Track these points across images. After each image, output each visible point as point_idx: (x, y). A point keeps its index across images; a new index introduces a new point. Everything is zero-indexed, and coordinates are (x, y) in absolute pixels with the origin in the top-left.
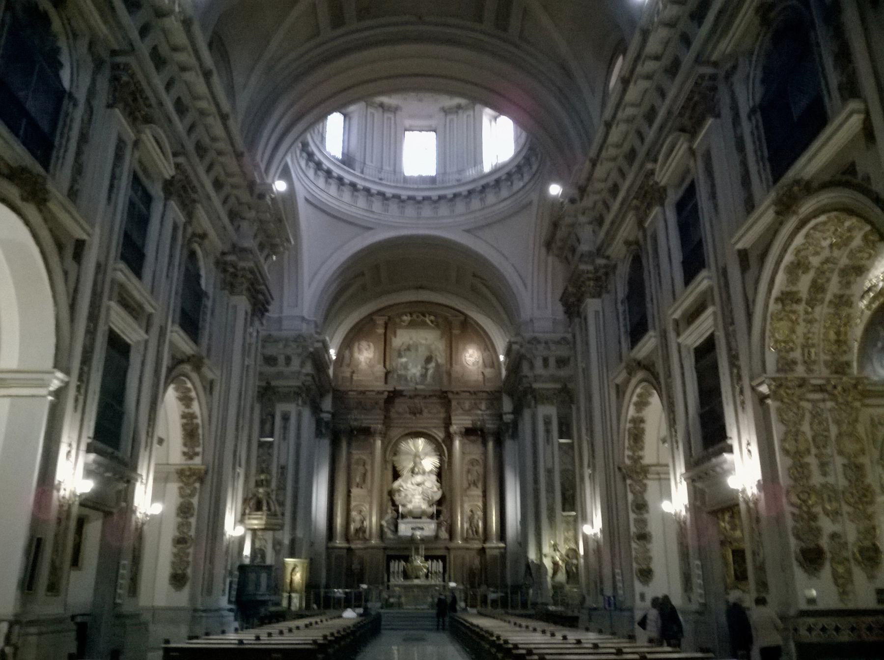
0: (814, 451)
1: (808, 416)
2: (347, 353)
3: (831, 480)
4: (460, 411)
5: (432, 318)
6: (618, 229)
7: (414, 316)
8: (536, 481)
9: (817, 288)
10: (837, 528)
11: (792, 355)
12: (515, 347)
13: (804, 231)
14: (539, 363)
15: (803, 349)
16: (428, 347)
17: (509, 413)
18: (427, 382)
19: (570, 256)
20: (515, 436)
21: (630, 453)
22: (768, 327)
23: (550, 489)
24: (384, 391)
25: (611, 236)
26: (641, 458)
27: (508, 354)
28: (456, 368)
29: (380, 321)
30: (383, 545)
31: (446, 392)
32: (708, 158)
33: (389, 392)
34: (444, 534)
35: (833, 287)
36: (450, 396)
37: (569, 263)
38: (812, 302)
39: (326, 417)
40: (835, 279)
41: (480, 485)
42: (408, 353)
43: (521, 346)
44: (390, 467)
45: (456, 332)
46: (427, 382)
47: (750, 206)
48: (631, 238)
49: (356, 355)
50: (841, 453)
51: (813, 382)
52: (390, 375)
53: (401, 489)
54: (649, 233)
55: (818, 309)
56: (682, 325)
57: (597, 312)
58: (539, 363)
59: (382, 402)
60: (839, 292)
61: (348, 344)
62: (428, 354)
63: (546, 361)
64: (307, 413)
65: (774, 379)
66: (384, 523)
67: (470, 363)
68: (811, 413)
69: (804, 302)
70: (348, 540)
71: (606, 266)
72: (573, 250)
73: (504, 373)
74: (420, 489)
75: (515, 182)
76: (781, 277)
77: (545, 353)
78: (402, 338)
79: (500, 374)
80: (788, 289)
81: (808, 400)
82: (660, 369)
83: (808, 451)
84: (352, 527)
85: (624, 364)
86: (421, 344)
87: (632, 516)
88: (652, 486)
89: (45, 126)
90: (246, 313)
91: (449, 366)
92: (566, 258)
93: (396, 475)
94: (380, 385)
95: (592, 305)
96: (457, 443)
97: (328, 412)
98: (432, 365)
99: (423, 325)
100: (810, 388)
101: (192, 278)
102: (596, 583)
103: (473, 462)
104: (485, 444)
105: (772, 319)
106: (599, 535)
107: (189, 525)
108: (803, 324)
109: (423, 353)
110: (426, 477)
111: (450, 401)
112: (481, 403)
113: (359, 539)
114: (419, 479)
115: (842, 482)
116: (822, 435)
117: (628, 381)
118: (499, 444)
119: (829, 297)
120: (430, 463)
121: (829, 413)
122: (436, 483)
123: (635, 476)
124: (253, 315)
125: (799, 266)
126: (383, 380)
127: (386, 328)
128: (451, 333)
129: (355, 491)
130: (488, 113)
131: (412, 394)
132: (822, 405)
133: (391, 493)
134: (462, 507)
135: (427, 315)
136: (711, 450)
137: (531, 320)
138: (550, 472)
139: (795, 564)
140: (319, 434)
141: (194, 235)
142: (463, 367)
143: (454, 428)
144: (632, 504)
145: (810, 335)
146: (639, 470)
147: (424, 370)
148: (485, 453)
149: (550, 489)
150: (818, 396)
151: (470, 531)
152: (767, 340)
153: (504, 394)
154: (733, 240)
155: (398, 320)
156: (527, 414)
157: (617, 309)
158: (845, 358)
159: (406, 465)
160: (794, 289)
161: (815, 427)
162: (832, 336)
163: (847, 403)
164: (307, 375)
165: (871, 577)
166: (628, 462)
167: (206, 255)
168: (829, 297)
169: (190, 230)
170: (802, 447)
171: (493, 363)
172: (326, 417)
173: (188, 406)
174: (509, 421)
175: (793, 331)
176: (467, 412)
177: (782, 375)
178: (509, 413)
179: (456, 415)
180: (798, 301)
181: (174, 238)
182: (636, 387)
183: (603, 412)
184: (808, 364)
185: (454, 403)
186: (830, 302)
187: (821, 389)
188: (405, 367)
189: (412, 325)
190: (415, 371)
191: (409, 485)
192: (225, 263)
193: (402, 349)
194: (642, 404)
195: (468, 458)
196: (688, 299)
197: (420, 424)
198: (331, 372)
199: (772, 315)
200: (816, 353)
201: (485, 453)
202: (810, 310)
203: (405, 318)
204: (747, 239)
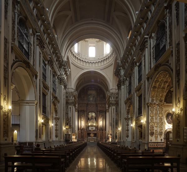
0: (155, 116)
10: (157, 129)
50: (159, 116)
57: (123, 88)
83: (154, 116)
88: (130, 121)
138: (114, 118)
156: (110, 107)
165: (161, 137)
170: (153, 115)
187: (158, 105)
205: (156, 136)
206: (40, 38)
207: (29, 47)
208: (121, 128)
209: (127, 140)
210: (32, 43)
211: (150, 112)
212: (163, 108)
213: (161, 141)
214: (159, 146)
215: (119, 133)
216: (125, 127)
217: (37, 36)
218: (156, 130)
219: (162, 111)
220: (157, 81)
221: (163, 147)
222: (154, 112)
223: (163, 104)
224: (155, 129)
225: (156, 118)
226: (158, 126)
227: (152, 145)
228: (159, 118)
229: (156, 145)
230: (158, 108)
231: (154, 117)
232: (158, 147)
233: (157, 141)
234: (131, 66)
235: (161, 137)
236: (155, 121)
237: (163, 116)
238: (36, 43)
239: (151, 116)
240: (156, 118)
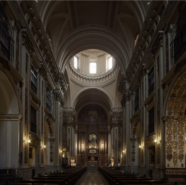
0: (173, 133)
3: (176, 140)
10: (175, 151)
34: (97, 153)
50: (178, 134)
107: (52, 150)
115: (178, 141)
139: (166, 158)
150: (176, 121)
165: (181, 161)
170: (171, 133)
205: (175, 160)
206: (27, 35)
211: (167, 128)
212: (184, 123)
214: (180, 174)
217: (22, 33)
218: (175, 152)
219: (183, 126)
222: (172, 128)
223: (184, 118)
224: (173, 150)
225: (175, 136)
226: (178, 146)
227: (170, 172)
228: (178, 136)
229: (176, 172)
230: (178, 123)
231: (171, 135)
232: (178, 174)
233: (176, 167)
235: (181, 161)
236: (173, 140)
237: (183, 133)
238: (21, 41)
239: (167, 134)
240: (175, 136)
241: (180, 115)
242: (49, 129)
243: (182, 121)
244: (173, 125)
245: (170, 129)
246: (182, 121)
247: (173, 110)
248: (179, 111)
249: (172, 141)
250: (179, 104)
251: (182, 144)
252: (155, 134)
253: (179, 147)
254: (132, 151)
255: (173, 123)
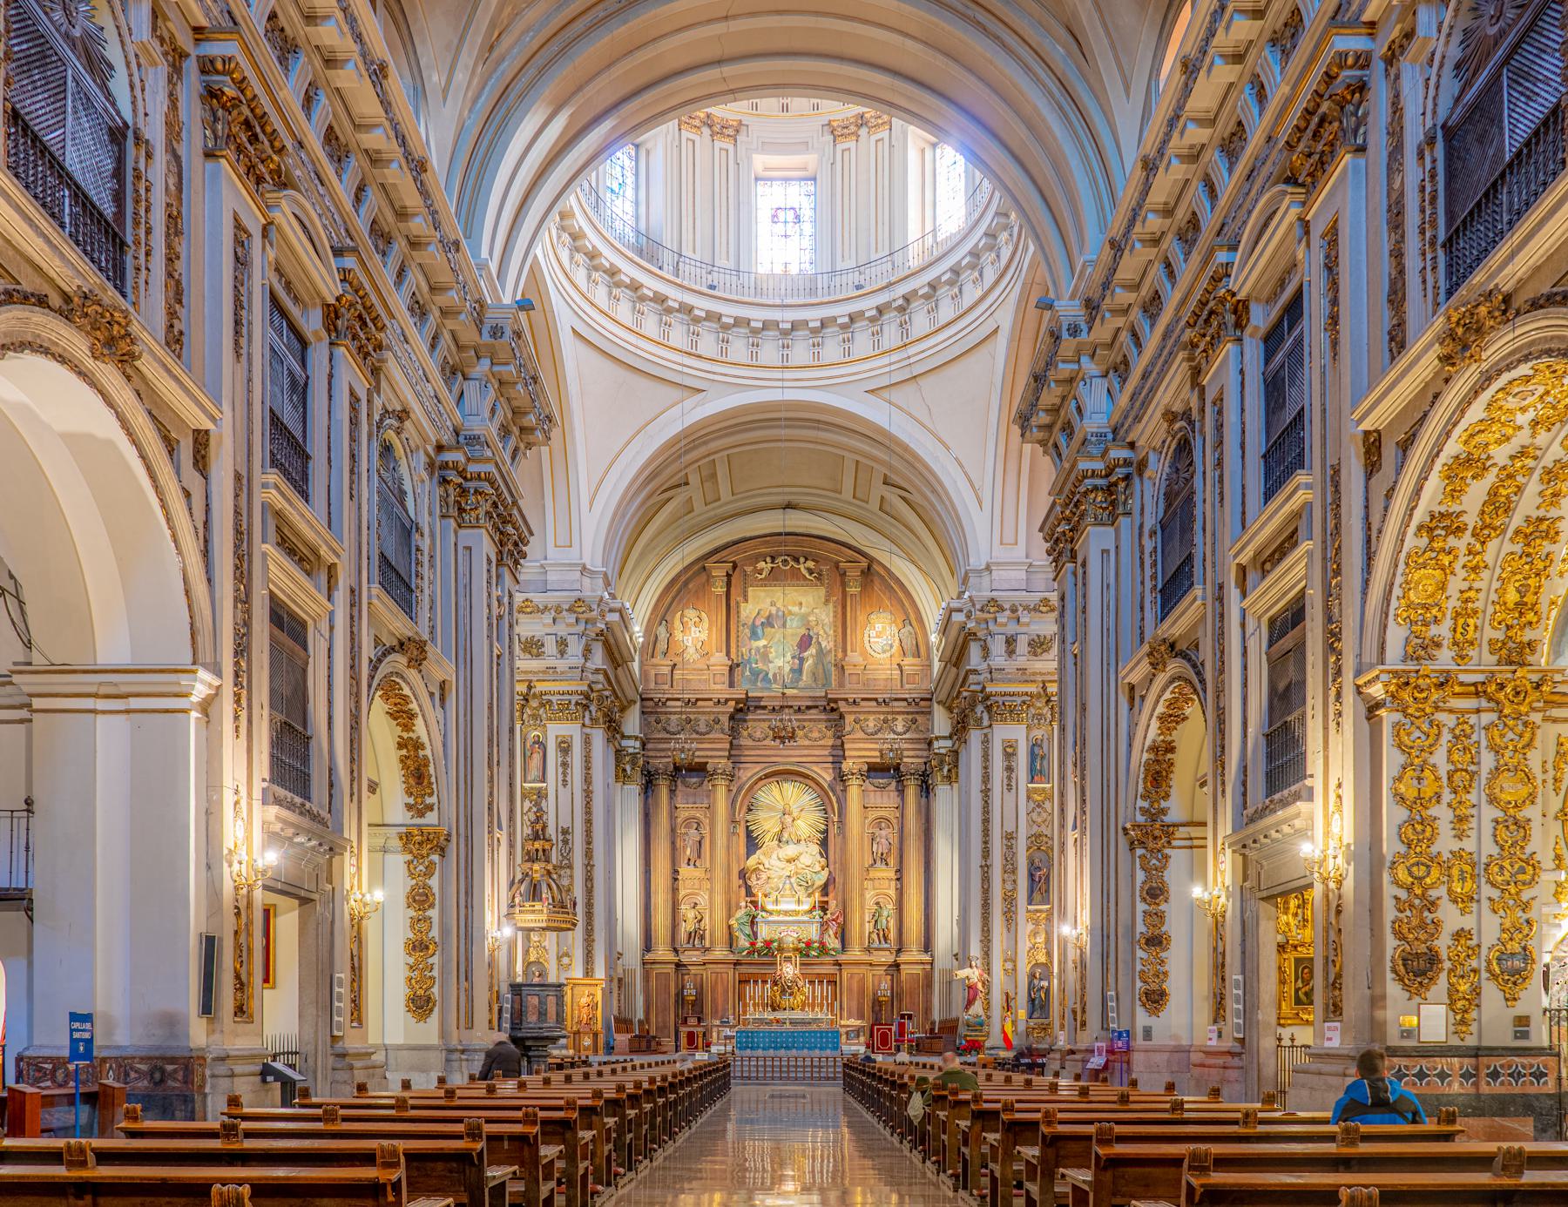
0: (1447, 796)
1: (1446, 736)
2: (662, 632)
3: (1469, 845)
4: (860, 735)
5: (810, 564)
6: (1153, 390)
7: (779, 560)
8: (986, 853)
9: (1497, 504)
10: (1468, 922)
11: (1434, 630)
12: (958, 618)
13: (1486, 396)
14: (997, 646)
15: (1455, 619)
16: (804, 618)
17: (944, 738)
18: (801, 684)
19: (1062, 442)
20: (949, 779)
21: (1146, 804)
22: (1399, 580)
23: (1010, 868)
24: (727, 700)
25: (1141, 401)
26: (1164, 812)
27: (944, 630)
28: (854, 657)
29: (719, 572)
30: (731, 957)
31: (835, 701)
32: (1332, 237)
33: (738, 701)
35: (1528, 505)
36: (843, 707)
37: (1059, 455)
38: (1483, 534)
39: (632, 746)
40: (1533, 486)
41: (892, 861)
42: (768, 630)
43: (968, 617)
44: (741, 831)
45: (853, 589)
46: (801, 684)
47: (1397, 341)
48: (1178, 407)
49: (678, 635)
50: (1493, 800)
51: (1463, 678)
52: (738, 671)
53: (761, 867)
54: (1210, 396)
55: (1492, 546)
56: (1252, 576)
57: (1105, 552)
58: (997, 646)
59: (725, 719)
60: (1535, 514)
61: (663, 613)
62: (803, 631)
63: (1010, 642)
64: (598, 736)
65: (1396, 674)
66: (732, 922)
67: (878, 648)
68: (1452, 730)
69: (1468, 533)
70: (676, 951)
71: (1127, 463)
72: (1068, 429)
73: (937, 666)
74: (792, 867)
75: (968, 288)
76: (1434, 483)
77: (1012, 628)
78: (757, 602)
79: (930, 666)
80: (1443, 509)
81: (1451, 711)
82: (1206, 654)
83: (1438, 796)
84: (685, 928)
85: (1146, 648)
86: (790, 613)
87: (1141, 907)
88: (1178, 858)
89: (108, 210)
90: (489, 561)
91: (840, 655)
92: (1056, 446)
93: (752, 844)
94: (720, 689)
95: (1096, 540)
96: (854, 791)
97: (636, 738)
98: (812, 650)
99: (796, 575)
100: (1457, 689)
101: (393, 496)
102: (1074, 1012)
103: (880, 822)
104: (901, 792)
105: (1407, 564)
106: (1086, 938)
108: (1462, 573)
109: (795, 629)
110: (802, 847)
111: (842, 717)
112: (895, 720)
113: (694, 948)
114: (790, 850)
115: (1489, 848)
116: (1466, 771)
117: (1151, 679)
118: (926, 789)
119: (1517, 521)
120: (807, 822)
121: (1483, 732)
122: (818, 856)
123: (1151, 845)
124: (500, 562)
125: (1470, 464)
126: (726, 679)
127: (729, 585)
128: (844, 594)
129: (685, 871)
130: (915, 137)
131: (777, 704)
132: (1473, 719)
133: (743, 874)
134: (862, 895)
135: (802, 560)
136: (1277, 797)
137: (988, 568)
138: (1010, 837)
140: (622, 776)
141: (386, 412)
142: (864, 654)
143: (847, 765)
144: (1141, 891)
145: (1472, 594)
146: (1157, 833)
147: (797, 661)
148: (901, 808)
149: (1010, 868)
150: (1470, 703)
151: (874, 936)
152: (1394, 603)
153: (936, 705)
154: (1356, 416)
155: (749, 569)
156: (975, 737)
157: (1141, 547)
158: (1528, 635)
159: (767, 823)
160: (1455, 508)
161: (1456, 757)
162: (1512, 596)
163: (1518, 716)
164: (597, 671)
165: (1511, 999)
166: (1140, 819)
167: (410, 451)
168: (1517, 521)
169: (378, 403)
170: (1428, 792)
171: (918, 649)
172: (632, 746)
173: (407, 728)
174: (943, 751)
175: (1443, 587)
176: (871, 736)
177: (1411, 666)
178: (944, 738)
179: (854, 741)
180: (1459, 530)
181: (354, 422)
182: (1163, 690)
183: (1104, 735)
184: (1461, 647)
185: (849, 719)
186: (1517, 532)
187: (1477, 691)
188: (765, 656)
189: (774, 577)
190: (780, 661)
191: (774, 861)
192: (445, 466)
193: (758, 623)
194: (1172, 719)
195: (873, 815)
196: (1267, 525)
197: (788, 756)
198: (636, 666)
199: (1409, 556)
200: (1476, 627)
201: (901, 808)
202: (1478, 546)
203: (761, 565)
204: (1381, 414)
205: (1464, 987)
206: (241, 84)
207: (118, 174)
208: (1085, 917)
209: (1148, 1033)
210: (155, 132)
212: (1536, 717)
213: (1525, 1035)
214: (1496, 1088)
215: (1062, 971)
216: (1124, 916)
217: (203, 72)
218: (1459, 935)
219: (1528, 745)
220: (1470, 464)
221: (1533, 1090)
222: (1439, 758)
223: (1538, 686)
224: (1451, 917)
225: (1461, 819)
226: (1487, 891)
227: (1421, 1075)
228: (1489, 813)
229: (1466, 1076)
230: (1487, 718)
231: (1434, 811)
232: (1485, 1089)
233: (1471, 1041)
234: (1189, 334)
235: (1511, 999)
236: (1445, 843)
237: (1532, 798)
238: (194, 139)
239: (1400, 798)
240: (1461, 819)
241: (1511, 663)
242: (403, 760)
243: (1524, 709)
244: (1446, 736)
245: (1425, 761)
246: (1524, 709)
247: (1448, 623)
248: (1500, 635)
249: (1434, 850)
250: (1496, 585)
251: (1522, 871)
252: (1310, 798)
253: (1495, 894)
254: (1140, 928)
255: (1448, 720)
